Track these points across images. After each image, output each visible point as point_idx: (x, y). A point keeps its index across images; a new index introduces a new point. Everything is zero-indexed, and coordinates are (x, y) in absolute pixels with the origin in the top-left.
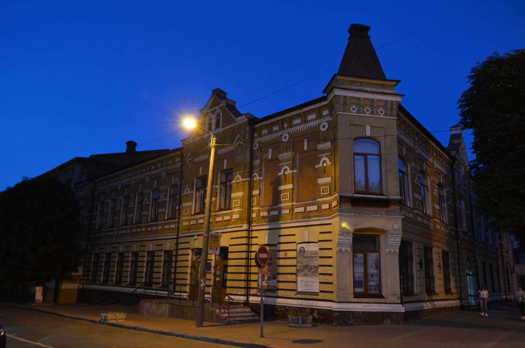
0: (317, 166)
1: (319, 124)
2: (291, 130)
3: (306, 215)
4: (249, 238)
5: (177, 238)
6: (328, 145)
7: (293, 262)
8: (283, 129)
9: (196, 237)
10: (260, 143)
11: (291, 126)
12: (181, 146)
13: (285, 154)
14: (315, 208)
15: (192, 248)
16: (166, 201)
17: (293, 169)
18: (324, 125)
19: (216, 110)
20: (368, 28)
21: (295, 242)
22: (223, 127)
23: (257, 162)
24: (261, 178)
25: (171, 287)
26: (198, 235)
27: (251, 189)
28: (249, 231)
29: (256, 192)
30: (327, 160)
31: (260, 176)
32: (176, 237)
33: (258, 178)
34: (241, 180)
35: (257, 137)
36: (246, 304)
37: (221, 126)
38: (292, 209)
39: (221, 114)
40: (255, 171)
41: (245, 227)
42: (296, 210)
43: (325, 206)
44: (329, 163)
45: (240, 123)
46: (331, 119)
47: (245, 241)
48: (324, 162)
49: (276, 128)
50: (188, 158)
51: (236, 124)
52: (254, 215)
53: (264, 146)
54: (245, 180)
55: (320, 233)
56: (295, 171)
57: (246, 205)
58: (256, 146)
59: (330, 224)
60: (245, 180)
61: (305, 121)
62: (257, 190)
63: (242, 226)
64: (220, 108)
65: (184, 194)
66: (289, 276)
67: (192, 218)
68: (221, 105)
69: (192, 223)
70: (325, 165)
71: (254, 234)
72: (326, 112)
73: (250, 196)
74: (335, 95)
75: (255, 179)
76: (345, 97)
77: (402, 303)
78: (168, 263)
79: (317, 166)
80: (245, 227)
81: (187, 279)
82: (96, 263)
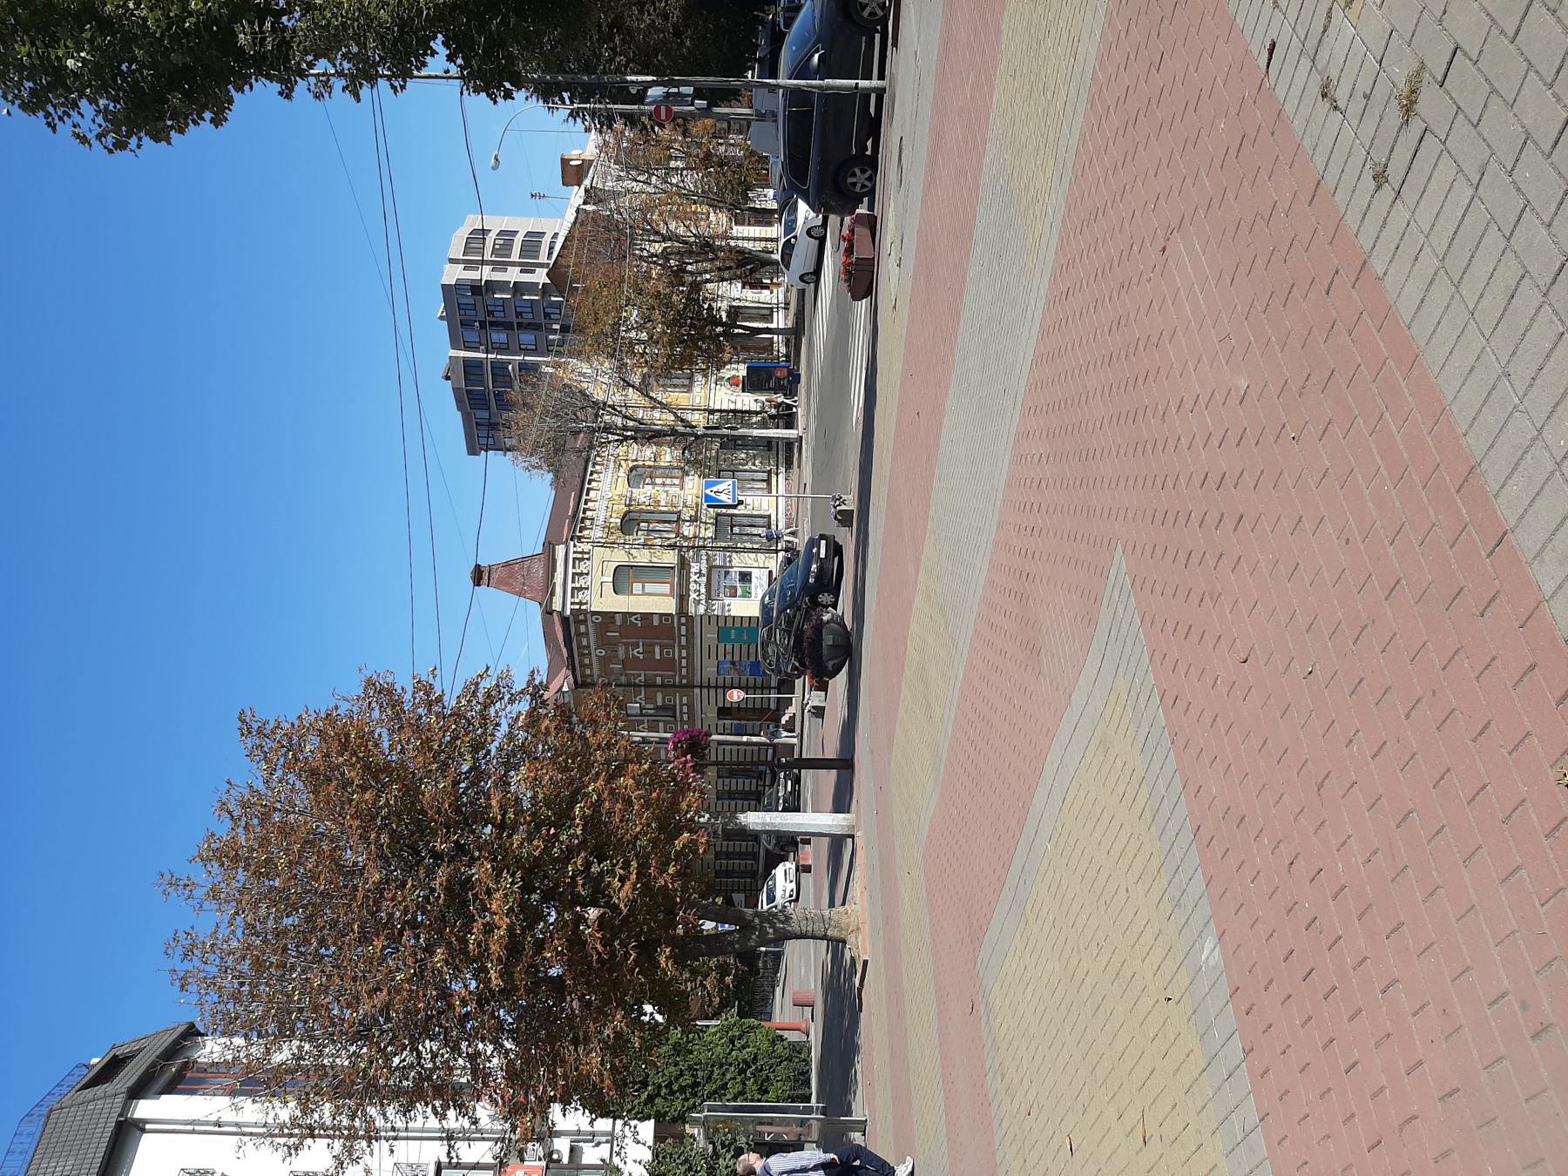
3: (690, 635)
4: (709, 687)
7: (737, 646)
11: (588, 646)
20: (478, 567)
23: (623, 679)
25: (761, 768)
28: (701, 687)
29: (659, 680)
41: (697, 691)
47: (712, 691)
53: (605, 670)
73: (663, 685)
77: (777, 551)
78: (732, 774)
80: (697, 691)
82: (728, 874)
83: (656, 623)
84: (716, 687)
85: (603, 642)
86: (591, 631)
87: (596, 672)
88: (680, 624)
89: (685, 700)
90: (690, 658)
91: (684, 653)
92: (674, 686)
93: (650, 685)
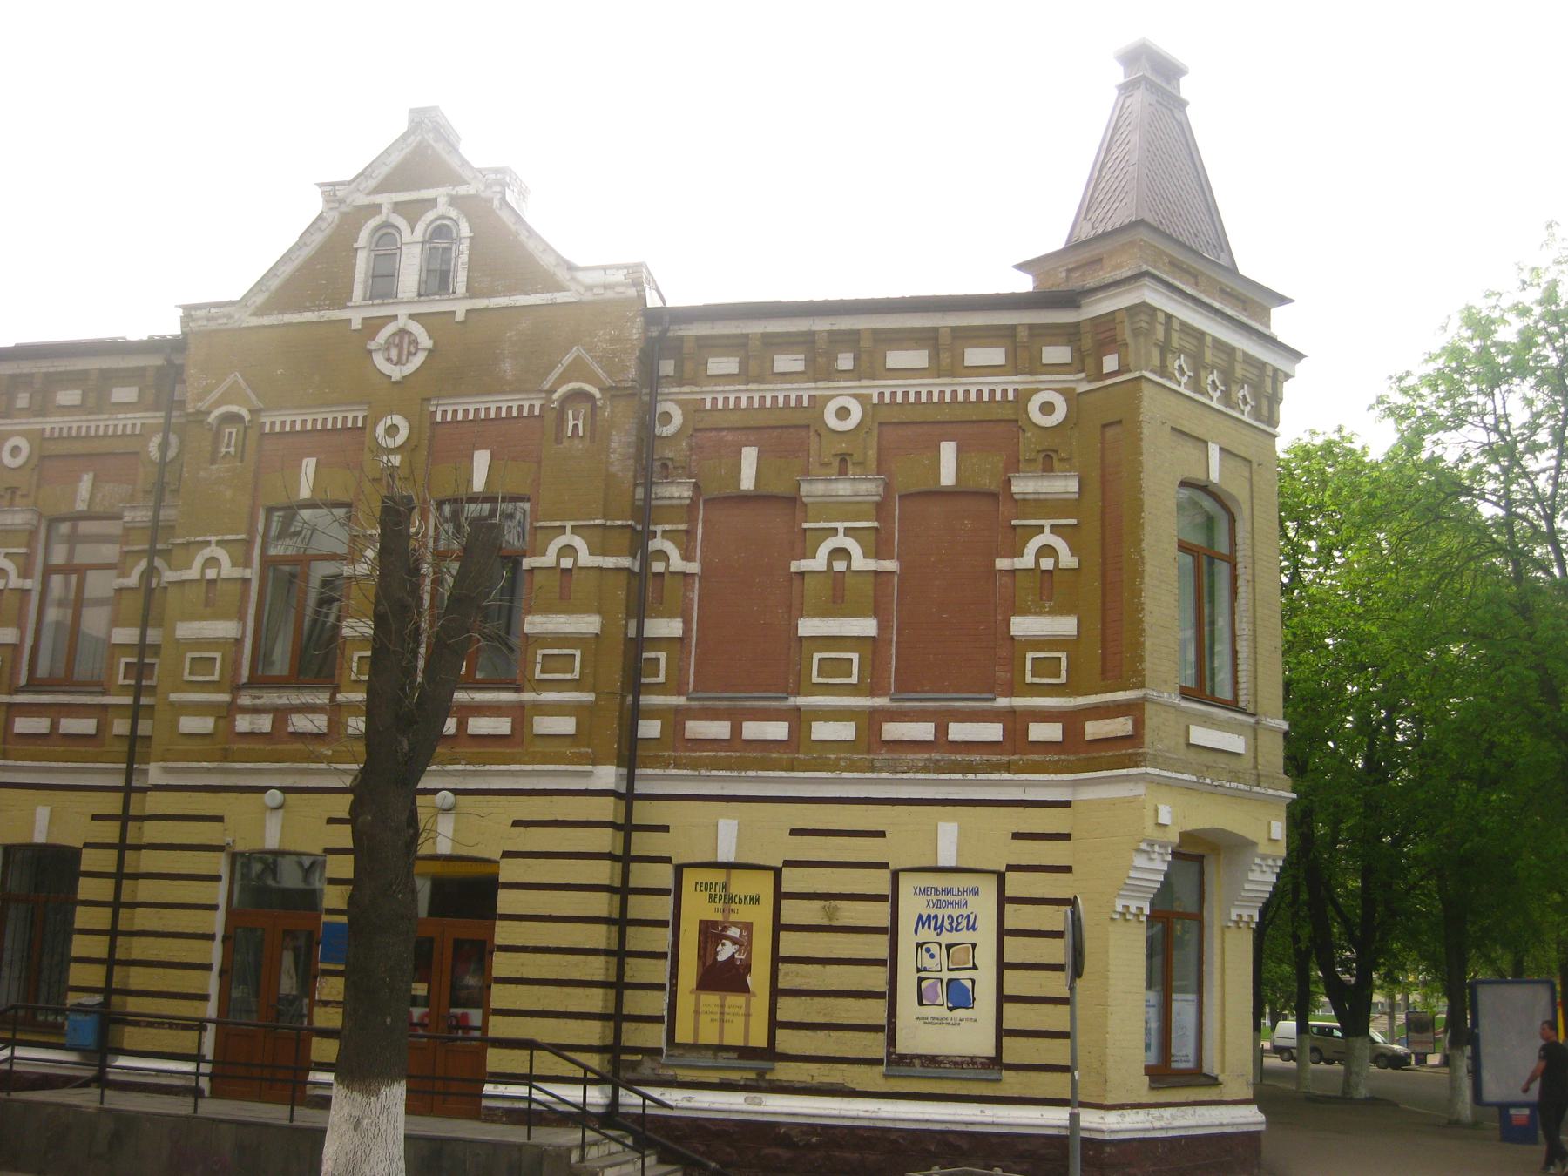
0: (1002, 564)
1: (1023, 397)
2: (873, 389)
3: (944, 755)
4: (626, 828)
5: (128, 790)
6: (1065, 486)
8: (831, 374)
9: (274, 797)
10: (693, 409)
12: (171, 327)
13: (843, 488)
14: (992, 732)
15: (239, 847)
16: (25, 593)
17: (878, 556)
18: (1048, 407)
19: (432, 203)
21: (885, 866)
22: (472, 293)
24: (694, 567)
26: (285, 790)
27: (639, 609)
28: (628, 797)
30: (1061, 546)
31: (687, 556)
32: (119, 781)
33: (677, 563)
34: (585, 559)
35: (679, 380)
36: (611, 1118)
37: (461, 289)
38: (870, 721)
39: (465, 230)
40: (659, 529)
41: (607, 776)
42: (893, 731)
43: (1040, 732)
44: (1067, 560)
45: (588, 297)
46: (1084, 387)
48: (1047, 551)
49: (786, 362)
50: (218, 403)
51: (560, 297)
52: (650, 729)
54: (609, 562)
55: (1017, 836)
56: (890, 565)
57: (614, 675)
58: (667, 417)
59: (1067, 804)
60: (609, 562)
61: (956, 369)
62: (671, 616)
63: (589, 774)
64: (454, 201)
65: (193, 573)
66: (850, 1002)
67: (245, 700)
68: (462, 190)
69: (243, 723)
70: (1046, 564)
71: (645, 813)
72: (1056, 354)
74: (1144, 304)
75: (658, 567)
76: (1169, 317)
79: (1002, 564)
80: (607, 776)
81: (205, 998)
83: (1023, 626)
84: (625, 859)
85: (901, 433)
86: (971, 386)
87: (715, 396)
88: (1016, 722)
89: (565, 725)
90: (798, 751)
91: (845, 731)
92: (634, 686)
93: (642, 592)
